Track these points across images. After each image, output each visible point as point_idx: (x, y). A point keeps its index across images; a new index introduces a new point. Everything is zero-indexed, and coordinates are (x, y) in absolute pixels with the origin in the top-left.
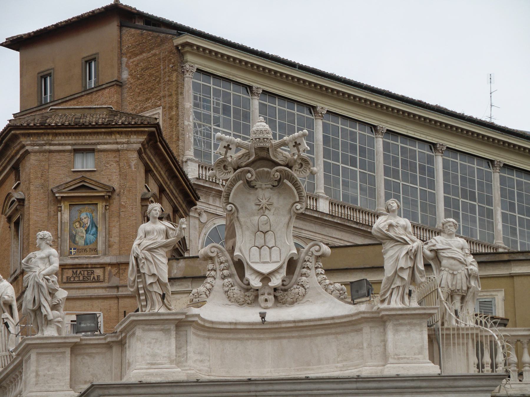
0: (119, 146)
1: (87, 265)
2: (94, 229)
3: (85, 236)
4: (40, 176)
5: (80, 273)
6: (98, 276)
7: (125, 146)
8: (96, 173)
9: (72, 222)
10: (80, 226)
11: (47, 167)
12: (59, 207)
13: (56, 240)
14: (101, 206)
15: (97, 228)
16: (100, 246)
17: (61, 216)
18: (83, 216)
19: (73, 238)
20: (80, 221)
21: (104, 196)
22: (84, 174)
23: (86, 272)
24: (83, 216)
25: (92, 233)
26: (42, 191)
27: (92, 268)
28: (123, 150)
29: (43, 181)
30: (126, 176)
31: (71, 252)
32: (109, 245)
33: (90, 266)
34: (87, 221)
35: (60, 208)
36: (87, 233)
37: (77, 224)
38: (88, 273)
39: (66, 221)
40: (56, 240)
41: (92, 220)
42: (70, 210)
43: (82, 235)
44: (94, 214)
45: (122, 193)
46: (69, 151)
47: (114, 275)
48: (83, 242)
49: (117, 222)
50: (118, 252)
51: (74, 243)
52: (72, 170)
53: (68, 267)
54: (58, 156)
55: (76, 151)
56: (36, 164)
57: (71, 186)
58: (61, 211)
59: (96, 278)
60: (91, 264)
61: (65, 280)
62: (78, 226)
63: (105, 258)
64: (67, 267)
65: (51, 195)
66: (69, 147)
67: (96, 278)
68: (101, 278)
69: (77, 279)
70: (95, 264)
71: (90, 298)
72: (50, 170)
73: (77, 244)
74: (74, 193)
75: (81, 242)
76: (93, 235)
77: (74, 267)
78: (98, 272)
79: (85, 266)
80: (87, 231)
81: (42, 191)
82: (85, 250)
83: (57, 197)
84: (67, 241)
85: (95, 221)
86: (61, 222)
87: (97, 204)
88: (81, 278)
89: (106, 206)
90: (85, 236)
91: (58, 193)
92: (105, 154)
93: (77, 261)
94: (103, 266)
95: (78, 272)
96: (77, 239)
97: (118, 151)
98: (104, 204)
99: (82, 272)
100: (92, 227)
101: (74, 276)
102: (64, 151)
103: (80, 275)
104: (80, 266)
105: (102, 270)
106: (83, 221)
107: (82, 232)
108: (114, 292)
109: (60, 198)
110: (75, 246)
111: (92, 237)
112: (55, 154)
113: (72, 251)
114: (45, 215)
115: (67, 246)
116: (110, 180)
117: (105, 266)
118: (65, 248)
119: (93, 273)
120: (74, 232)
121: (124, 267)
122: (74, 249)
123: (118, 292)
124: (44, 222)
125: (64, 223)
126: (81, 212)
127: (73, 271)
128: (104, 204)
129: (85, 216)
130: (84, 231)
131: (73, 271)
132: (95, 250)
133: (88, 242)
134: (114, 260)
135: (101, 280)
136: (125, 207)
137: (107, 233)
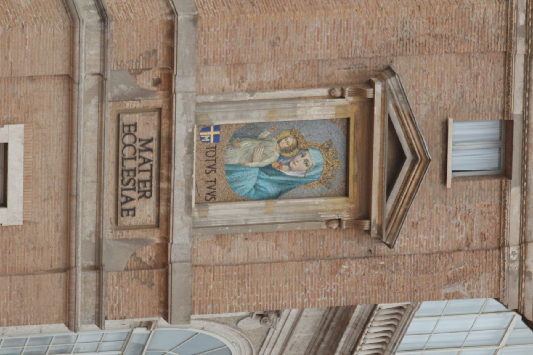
0: (513, 250)
1: (169, 179)
2: (272, 189)
3: (254, 164)
4: (438, 30)
5: (146, 161)
6: (134, 209)
7: (515, 266)
8: (438, 185)
9: (295, 128)
10: (285, 150)
11: (463, 48)
12: (343, 91)
13: (245, 86)
14: (342, 207)
15: (277, 196)
16: (220, 213)
17: (315, 98)
18: (315, 157)
19: (251, 132)
20: (300, 148)
21: (367, 216)
22: (435, 164)
23: (146, 176)
24: (315, 157)
25: (261, 183)
26: (394, 39)
27: (159, 190)
28: (502, 258)
29: (422, 40)
30: (426, 271)
31: (207, 129)
32: (221, 236)
33: (164, 185)
34: (296, 169)
35: (338, 93)
36: (262, 169)
37: (291, 141)
38: (144, 182)
39: (299, 113)
40: (245, 86)
41: (300, 183)
42: (331, 120)
43: (258, 156)
44: (318, 188)
45: (374, 261)
46: (506, 109)
47: (134, 254)
48: (236, 161)
49: (290, 253)
50: (200, 260)
51: (235, 135)
52: (451, 121)
53: (164, 127)
54: (493, 73)
55: (507, 126)
56: (473, 20)
57: (403, 125)
58: (331, 96)
59: (127, 206)
60: (169, 191)
61: (126, 119)
62: (284, 144)
63: (186, 230)
64: (165, 121)
65: (381, 64)
66: (517, 109)
67: (127, 206)
68: (127, 221)
69: (128, 152)
70: (168, 200)
71: (70, 194)
72: (454, 57)
73: (231, 144)
74: (383, 134)
75: (235, 156)
76: (256, 186)
77: (164, 142)
78: (146, 210)
79: (164, 172)
80: (268, 169)
81: (394, 39)
82: (212, 168)
83: (371, 84)
84: (241, 117)
85: (298, 190)
86: (299, 98)
87: (346, 194)
88: (130, 165)
89: (339, 220)
90: (254, 164)
91: (384, 92)
92: (494, 209)
93: (180, 149)
94: (163, 222)
95: (147, 155)
96: (246, 144)
97: (501, 246)
98: (345, 216)
99: (147, 166)
100: (280, 183)
101: (138, 145)
102: (507, 93)
103: (141, 161)
104: (164, 160)
105: (152, 220)
106: (299, 158)
107: (265, 156)
108: (83, 257)
109: (370, 96)
110: (225, 140)
111: (249, 184)
112: (500, 70)
113: (212, 133)
114: (322, 53)
115: (225, 118)
116: (415, 225)
117: (163, 225)
118: (220, 115)
119: (144, 195)
120: (266, 134)
121: (155, 280)
122: (217, 138)
123: (84, 269)
124: (301, 49)
125: (295, 108)
126: (325, 149)
127: (151, 140)
128: (345, 216)
129: (313, 162)
130: (267, 162)
131: (151, 140)
132: (211, 197)
133: (236, 175)
134: (176, 254)
135: (121, 219)
136: (333, 273)
137: (260, 229)
